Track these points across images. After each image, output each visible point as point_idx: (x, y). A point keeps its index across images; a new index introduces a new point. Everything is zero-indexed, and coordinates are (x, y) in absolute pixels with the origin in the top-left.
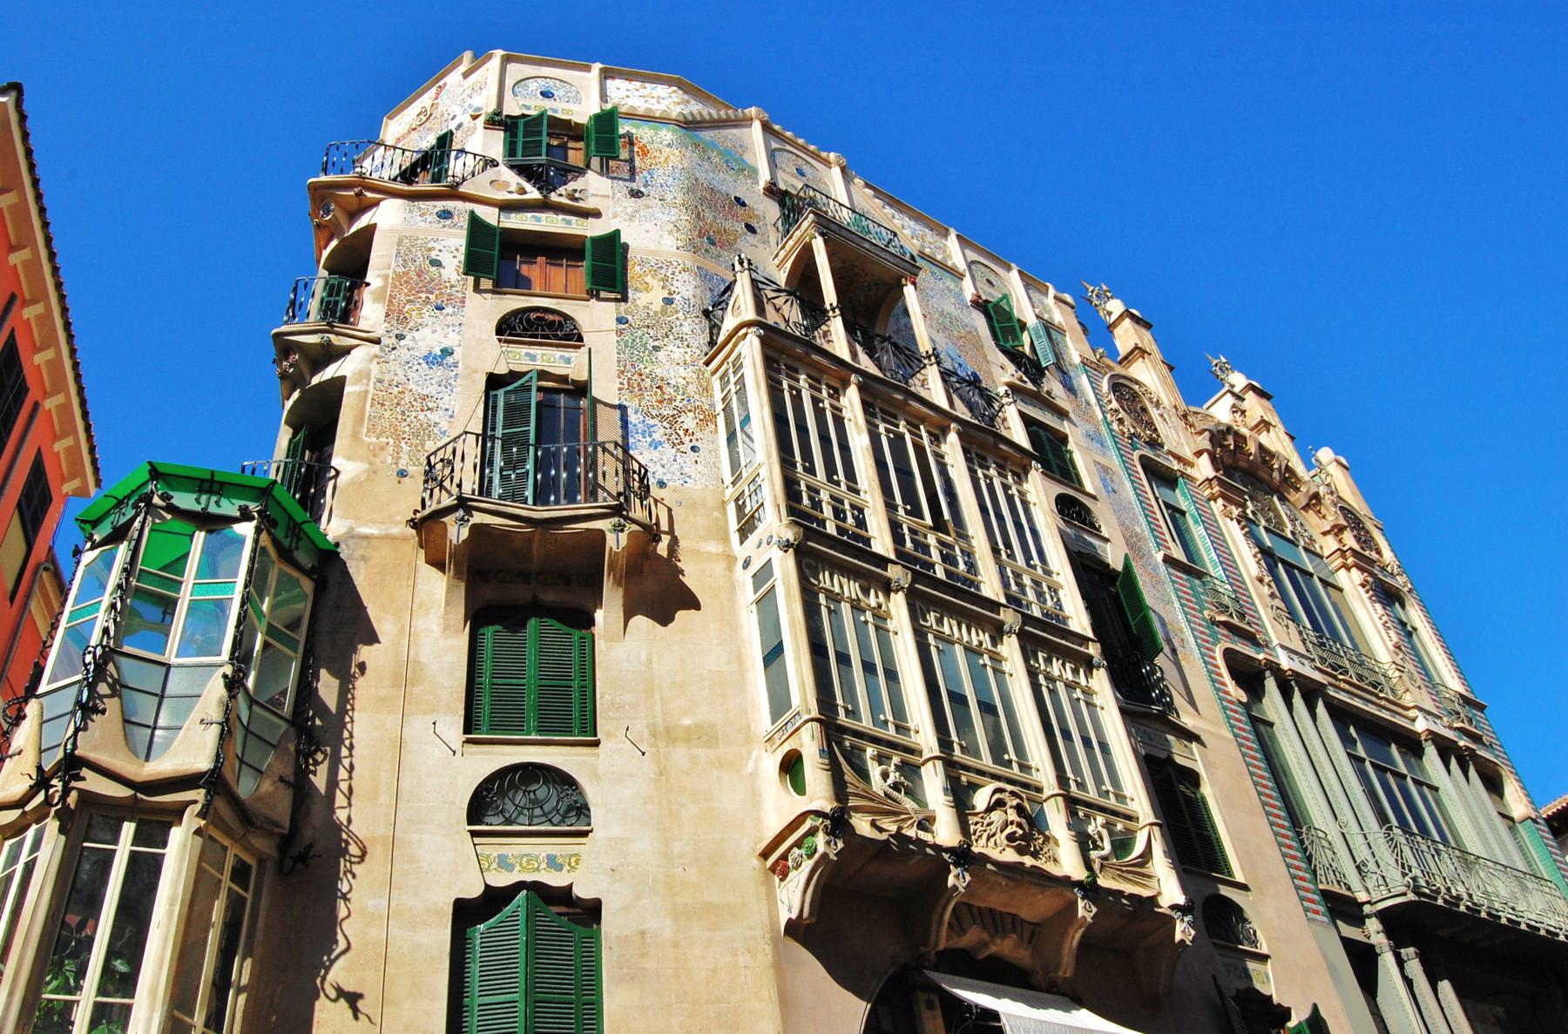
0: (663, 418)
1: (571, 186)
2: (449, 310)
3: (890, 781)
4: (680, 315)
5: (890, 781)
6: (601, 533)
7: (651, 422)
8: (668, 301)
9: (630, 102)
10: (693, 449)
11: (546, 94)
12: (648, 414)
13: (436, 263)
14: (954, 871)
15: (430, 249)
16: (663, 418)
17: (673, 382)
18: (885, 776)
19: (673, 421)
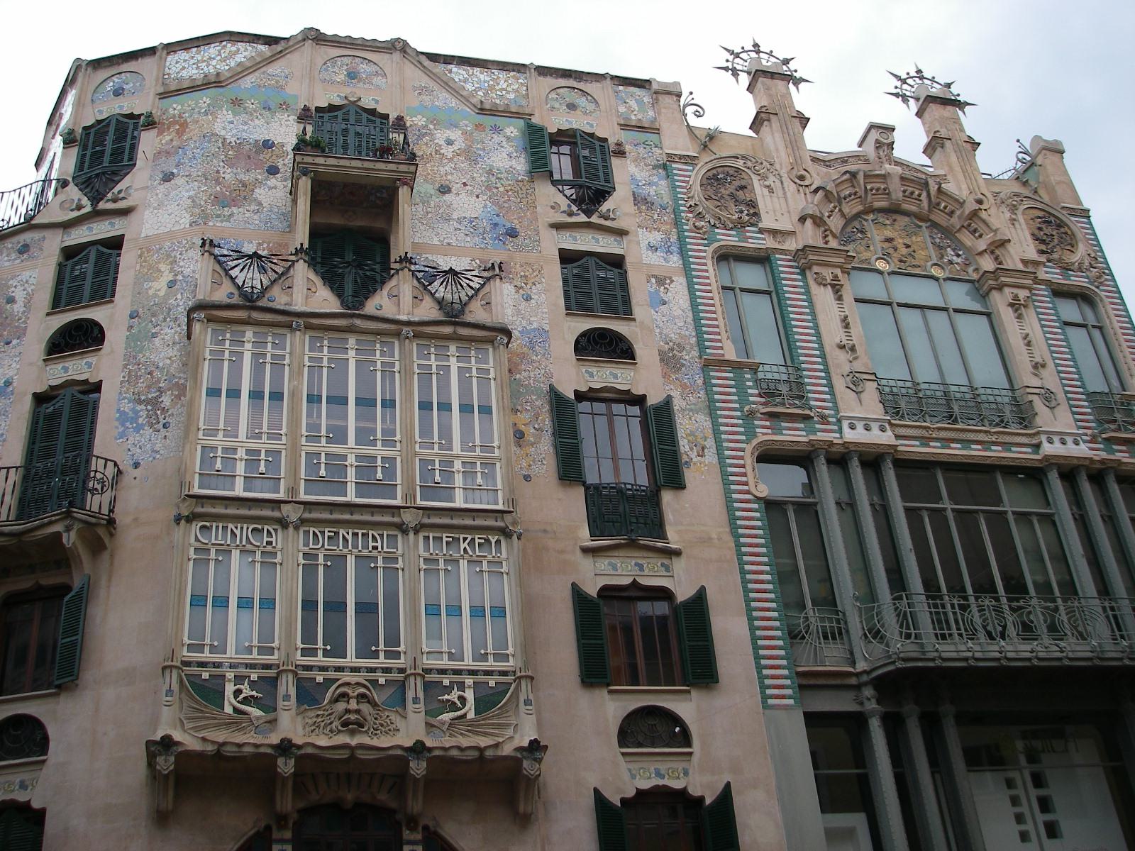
0: (148, 402)
1: (115, 190)
2: (15, 342)
3: (240, 698)
4: (179, 296)
5: (242, 696)
6: (58, 535)
7: (139, 408)
8: (171, 284)
9: (184, 74)
10: (165, 426)
11: (118, 93)
12: (140, 402)
13: (11, 300)
14: (281, 761)
15: (9, 288)
16: (148, 402)
17: (161, 365)
18: (237, 693)
19: (155, 403)
